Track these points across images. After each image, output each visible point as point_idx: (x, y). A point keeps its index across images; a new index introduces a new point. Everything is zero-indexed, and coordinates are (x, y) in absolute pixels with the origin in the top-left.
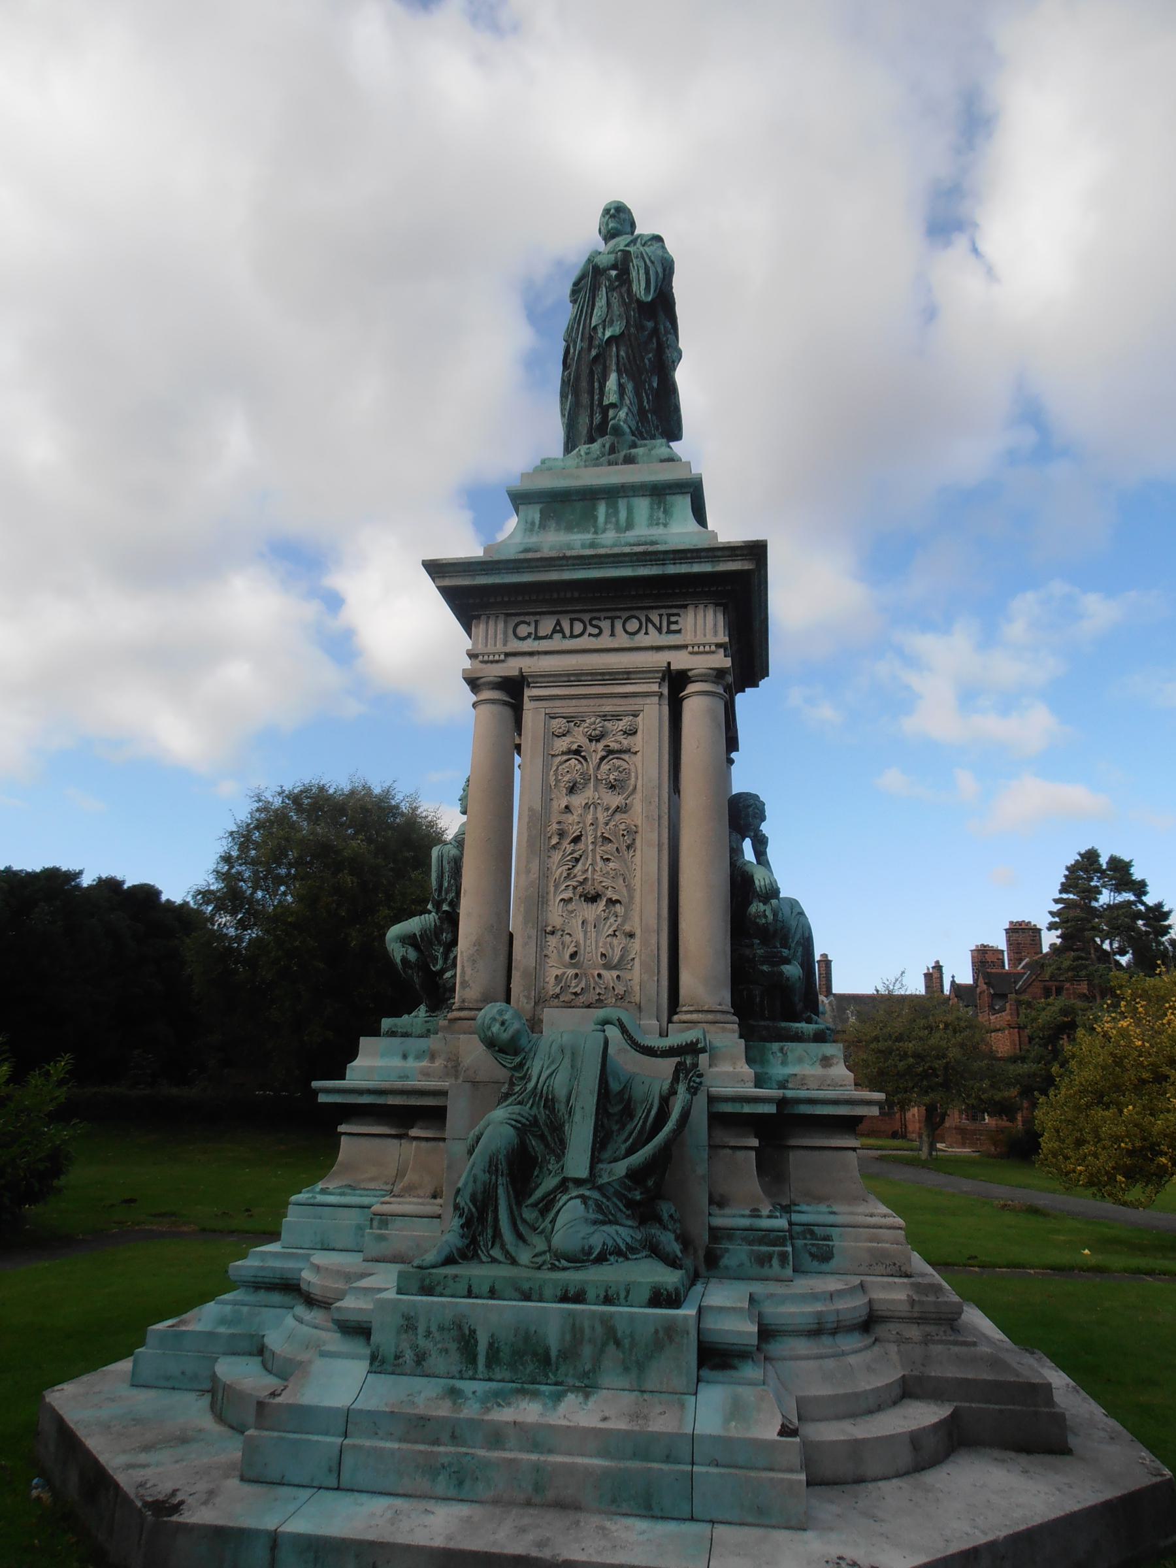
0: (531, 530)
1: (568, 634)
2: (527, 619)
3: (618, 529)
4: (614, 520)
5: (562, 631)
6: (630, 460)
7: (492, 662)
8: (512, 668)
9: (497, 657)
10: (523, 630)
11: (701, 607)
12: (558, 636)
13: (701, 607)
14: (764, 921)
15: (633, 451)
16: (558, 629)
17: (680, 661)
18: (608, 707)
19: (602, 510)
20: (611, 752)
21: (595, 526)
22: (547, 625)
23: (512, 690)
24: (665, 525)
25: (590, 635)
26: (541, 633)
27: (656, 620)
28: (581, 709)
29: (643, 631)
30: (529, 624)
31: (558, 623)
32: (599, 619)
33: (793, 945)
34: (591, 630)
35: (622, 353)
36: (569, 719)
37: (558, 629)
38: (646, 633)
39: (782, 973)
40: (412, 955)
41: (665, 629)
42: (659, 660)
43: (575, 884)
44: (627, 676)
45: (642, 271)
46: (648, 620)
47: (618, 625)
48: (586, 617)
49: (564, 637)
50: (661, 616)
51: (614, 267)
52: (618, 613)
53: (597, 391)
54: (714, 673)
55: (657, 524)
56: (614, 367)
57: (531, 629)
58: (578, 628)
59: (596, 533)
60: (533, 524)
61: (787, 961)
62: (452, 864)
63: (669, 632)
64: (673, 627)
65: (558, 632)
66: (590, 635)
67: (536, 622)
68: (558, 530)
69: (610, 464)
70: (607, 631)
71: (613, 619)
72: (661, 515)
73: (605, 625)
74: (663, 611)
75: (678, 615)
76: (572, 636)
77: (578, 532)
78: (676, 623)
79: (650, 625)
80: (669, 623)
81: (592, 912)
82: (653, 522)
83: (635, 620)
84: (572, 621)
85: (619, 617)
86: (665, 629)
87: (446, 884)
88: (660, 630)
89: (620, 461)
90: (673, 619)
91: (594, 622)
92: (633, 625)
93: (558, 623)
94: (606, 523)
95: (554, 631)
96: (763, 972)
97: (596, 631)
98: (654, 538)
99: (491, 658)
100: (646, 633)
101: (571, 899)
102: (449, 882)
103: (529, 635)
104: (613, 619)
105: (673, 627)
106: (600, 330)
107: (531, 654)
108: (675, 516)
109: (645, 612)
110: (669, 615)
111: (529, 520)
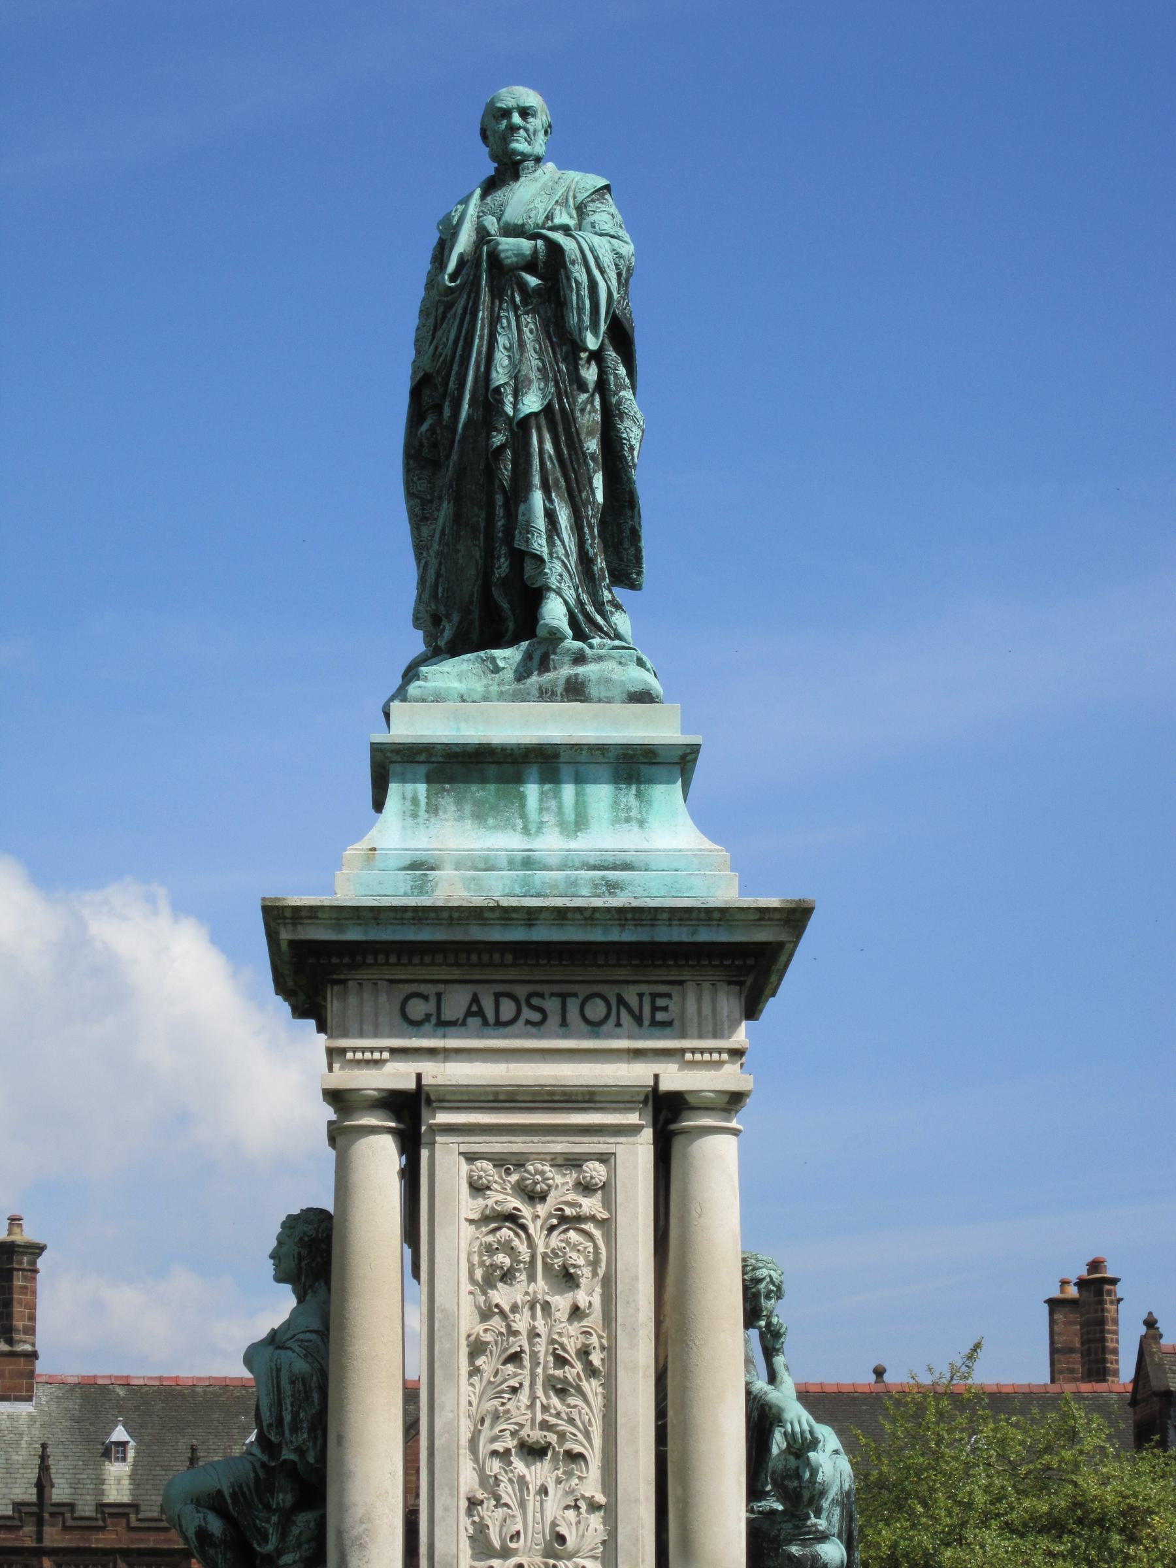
0: (415, 815)
1: (490, 1015)
2: (424, 988)
3: (562, 825)
4: (553, 804)
5: (481, 1013)
6: (576, 691)
7: (368, 1062)
8: (398, 1075)
9: (377, 1056)
10: (417, 1009)
11: (706, 985)
12: (474, 1022)
13: (706, 985)
14: (796, 1484)
15: (580, 670)
16: (474, 1010)
17: (673, 1078)
18: (561, 1146)
19: (532, 791)
20: (563, 1219)
21: (523, 816)
22: (456, 1002)
23: (408, 1112)
24: (641, 823)
25: (528, 1022)
26: (444, 1017)
27: (633, 1001)
28: (514, 1148)
29: (612, 1020)
30: (426, 998)
31: (475, 999)
32: (541, 996)
33: (825, 1504)
34: (527, 1014)
35: (549, 447)
36: (500, 1161)
37: (474, 1010)
38: (618, 1025)
39: (816, 1558)
40: (215, 1525)
41: (646, 1022)
42: (638, 1074)
43: (512, 1427)
44: (587, 1098)
45: (585, 292)
46: (621, 1001)
47: (573, 1006)
48: (521, 991)
49: (485, 1023)
50: (641, 996)
51: (531, 266)
52: (574, 988)
53: (500, 512)
54: (725, 1099)
55: (628, 820)
56: (537, 480)
57: (431, 1007)
58: (507, 1009)
59: (526, 831)
60: (415, 801)
61: (823, 1537)
62: (299, 1385)
63: (654, 1023)
64: (660, 1016)
65: (474, 1014)
66: (528, 1022)
67: (439, 996)
68: (460, 818)
69: (546, 694)
70: (554, 1019)
71: (563, 997)
72: (633, 802)
73: (552, 1005)
74: (644, 988)
75: (669, 996)
76: (499, 1023)
77: (495, 827)
78: (665, 1009)
79: (624, 1013)
80: (655, 1009)
81: (539, 1473)
82: (621, 817)
83: (599, 1001)
84: (498, 996)
85: (575, 995)
86: (646, 1022)
87: (288, 1418)
88: (638, 1019)
89: (560, 690)
90: (660, 1002)
91: (535, 1001)
92: (596, 1010)
93: (475, 999)
94: (541, 810)
95: (469, 1013)
96: (790, 1557)
97: (536, 1017)
98: (627, 857)
99: (368, 1056)
100: (618, 1025)
101: (507, 1451)
102: (295, 1416)
103: (428, 1017)
104: (563, 997)
105: (660, 1016)
106: (509, 399)
107: (432, 1052)
108: (656, 805)
109: (616, 989)
110: (654, 996)
111: (409, 795)
